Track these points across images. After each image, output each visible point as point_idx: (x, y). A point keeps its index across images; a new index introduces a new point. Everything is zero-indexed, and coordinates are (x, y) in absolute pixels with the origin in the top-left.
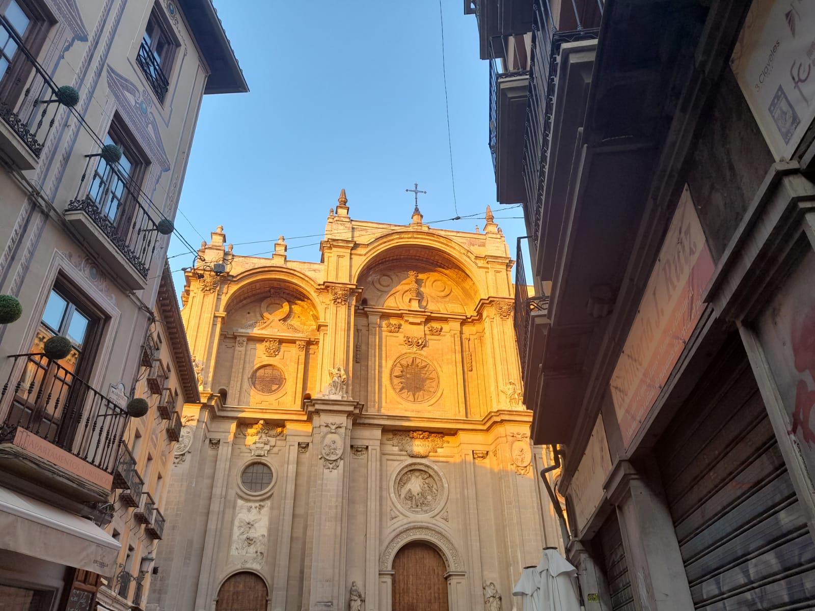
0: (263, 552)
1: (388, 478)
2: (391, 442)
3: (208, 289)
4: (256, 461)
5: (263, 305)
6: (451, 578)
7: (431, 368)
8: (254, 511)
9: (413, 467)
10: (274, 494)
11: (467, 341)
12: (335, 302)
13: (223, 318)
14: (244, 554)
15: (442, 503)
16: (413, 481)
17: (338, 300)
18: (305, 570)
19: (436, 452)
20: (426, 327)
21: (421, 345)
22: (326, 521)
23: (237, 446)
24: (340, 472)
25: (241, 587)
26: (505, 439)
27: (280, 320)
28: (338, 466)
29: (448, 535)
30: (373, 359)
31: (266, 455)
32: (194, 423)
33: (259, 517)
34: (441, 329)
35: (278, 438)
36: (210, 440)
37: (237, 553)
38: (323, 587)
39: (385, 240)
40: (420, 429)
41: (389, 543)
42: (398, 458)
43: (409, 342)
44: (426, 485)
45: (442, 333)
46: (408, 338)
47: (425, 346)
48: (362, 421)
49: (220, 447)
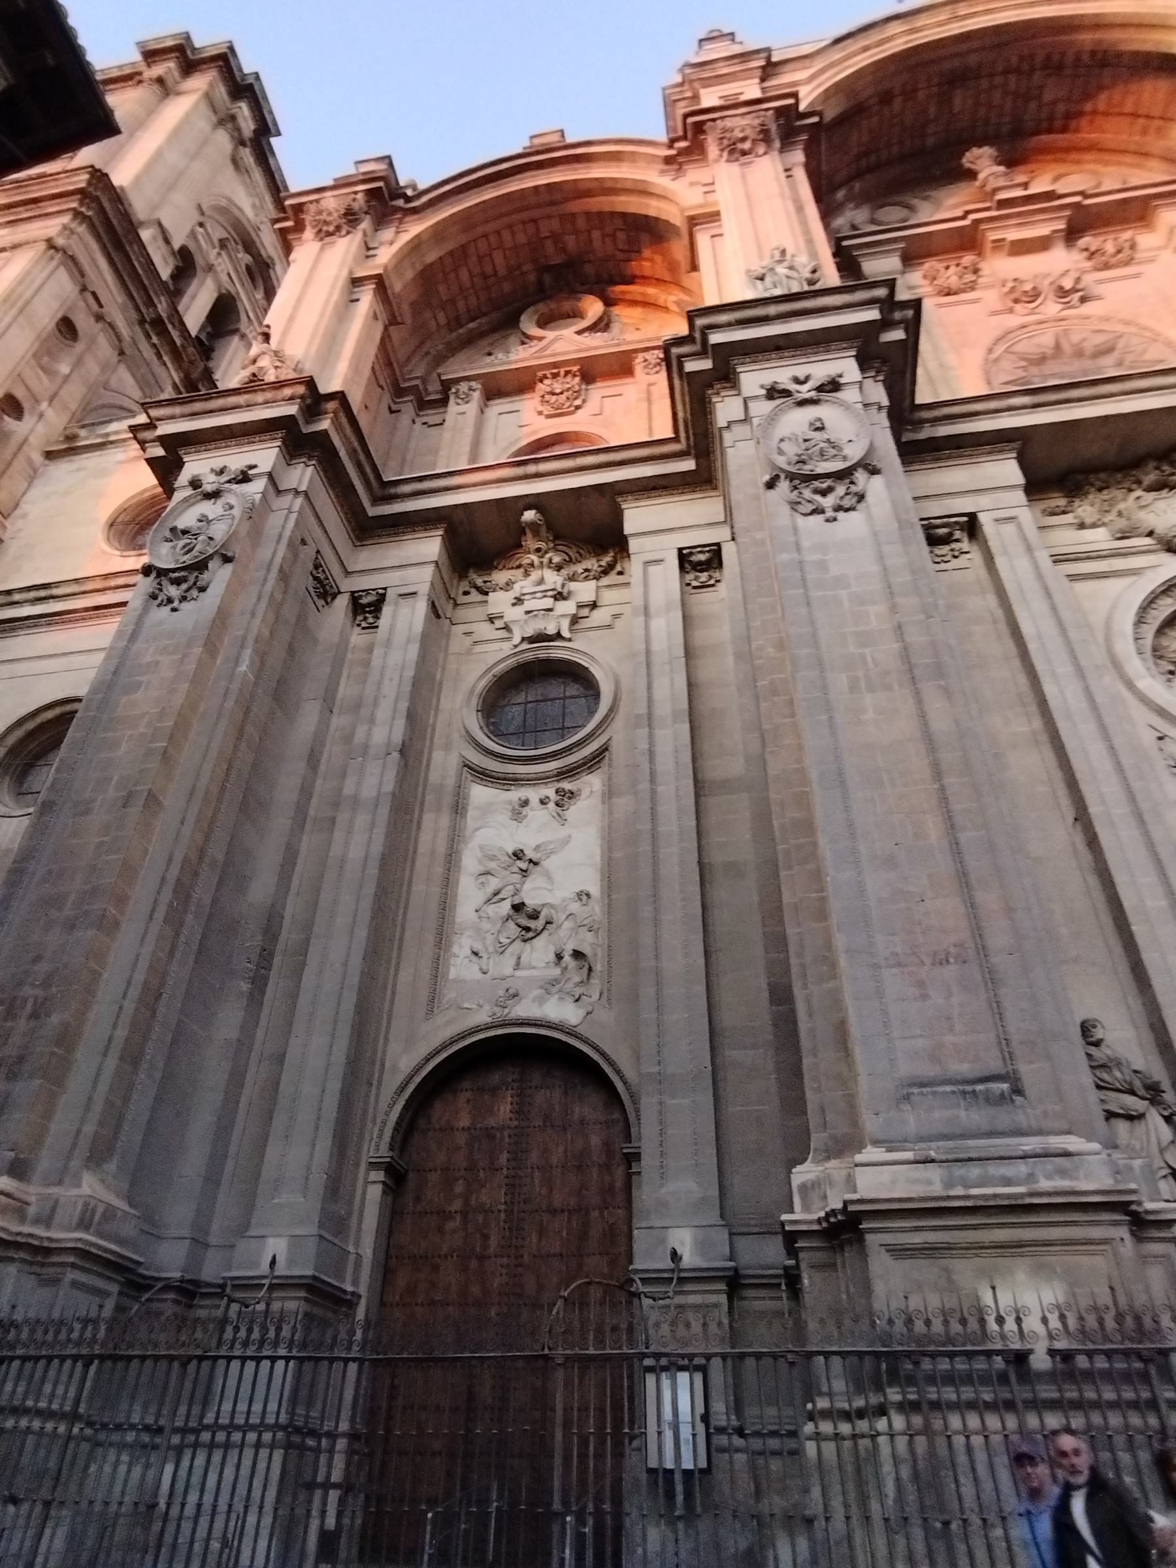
0: (587, 950)
2: (1069, 518)
3: (331, 228)
4: (529, 656)
5: (523, 318)
8: (538, 816)
10: (615, 747)
12: (732, 152)
13: (380, 281)
14: (508, 971)
17: (740, 146)
18: (791, 931)
21: (1074, 290)
22: (854, 687)
23: (460, 629)
24: (874, 510)
25: (504, 1109)
27: (579, 333)
28: (861, 497)
31: (566, 634)
32: (257, 487)
33: (562, 832)
35: (605, 581)
36: (355, 597)
37: (480, 976)
38: (925, 997)
39: (862, 42)
43: (1026, 292)
45: (1138, 256)
49: (387, 610)
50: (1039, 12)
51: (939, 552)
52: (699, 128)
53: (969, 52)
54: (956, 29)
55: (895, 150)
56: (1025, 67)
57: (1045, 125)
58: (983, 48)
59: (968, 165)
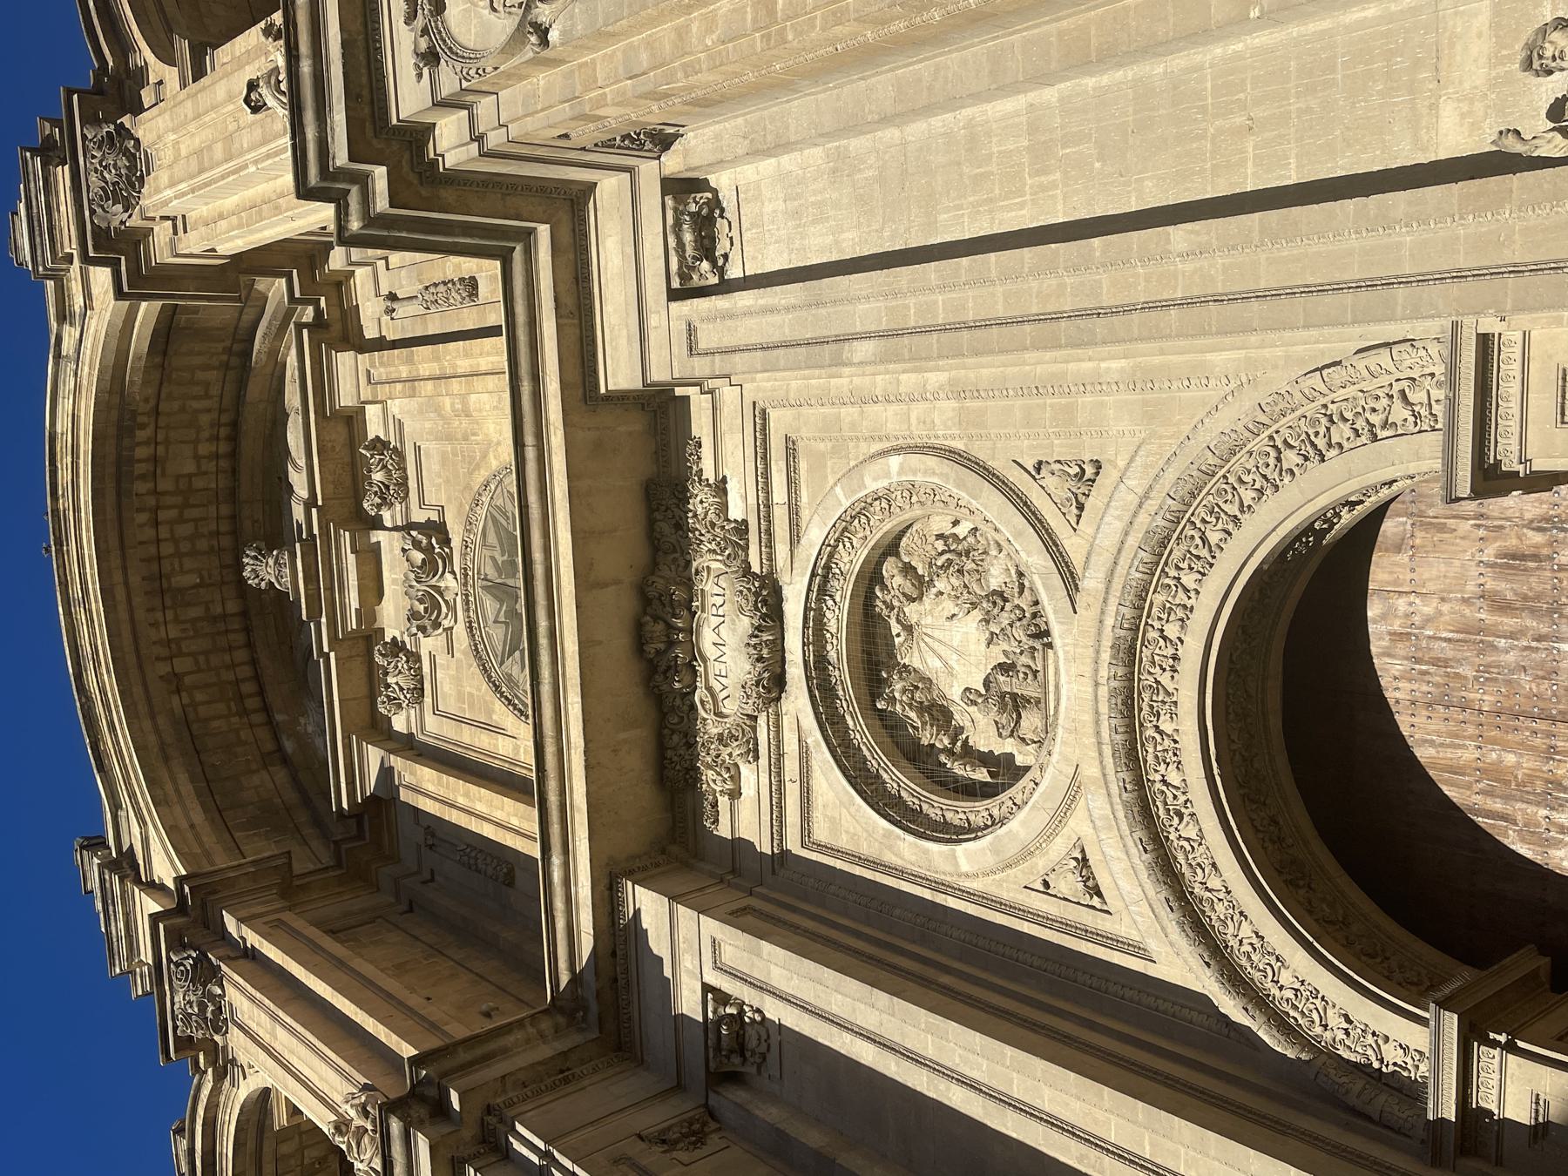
1: (889, 858)
2: (723, 801)
6: (1511, 464)
7: (499, 502)
9: (842, 675)
11: (402, 310)
12: (217, 1030)
15: (992, 504)
16: (935, 663)
17: (209, 1015)
19: (742, 528)
20: (387, 517)
26: (484, 107)
29: (1171, 475)
30: (480, 807)
34: (379, 445)
40: (618, 642)
41: (1235, 979)
42: (791, 767)
44: (940, 585)
46: (413, 615)
47: (438, 529)
48: (594, 1007)
50: (86, 502)
51: (754, 1043)
52: (185, 1043)
53: (126, 584)
54: (97, 606)
55: (241, 655)
56: (151, 501)
57: (224, 464)
58: (125, 568)
59: (263, 585)
